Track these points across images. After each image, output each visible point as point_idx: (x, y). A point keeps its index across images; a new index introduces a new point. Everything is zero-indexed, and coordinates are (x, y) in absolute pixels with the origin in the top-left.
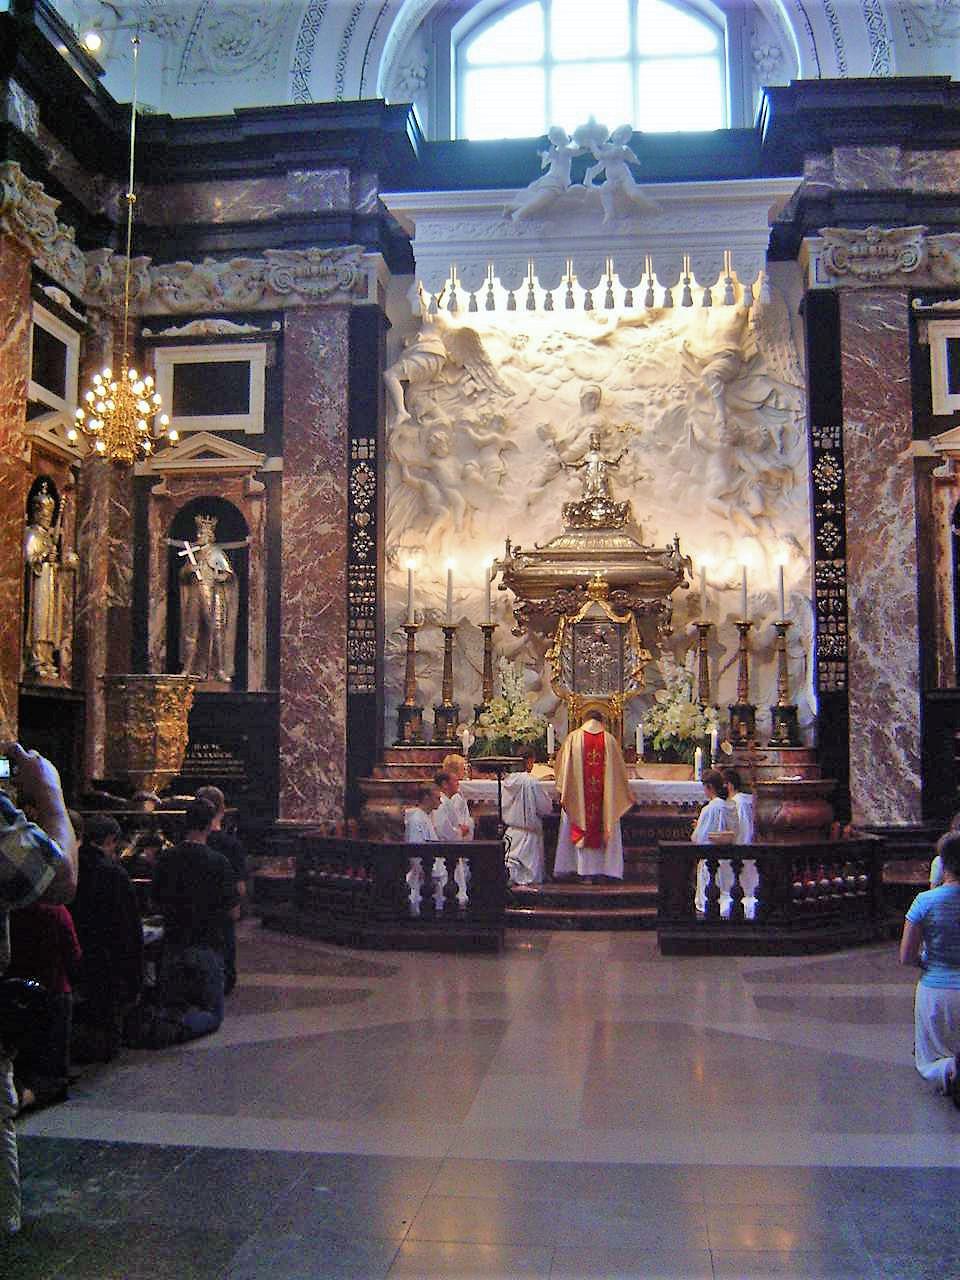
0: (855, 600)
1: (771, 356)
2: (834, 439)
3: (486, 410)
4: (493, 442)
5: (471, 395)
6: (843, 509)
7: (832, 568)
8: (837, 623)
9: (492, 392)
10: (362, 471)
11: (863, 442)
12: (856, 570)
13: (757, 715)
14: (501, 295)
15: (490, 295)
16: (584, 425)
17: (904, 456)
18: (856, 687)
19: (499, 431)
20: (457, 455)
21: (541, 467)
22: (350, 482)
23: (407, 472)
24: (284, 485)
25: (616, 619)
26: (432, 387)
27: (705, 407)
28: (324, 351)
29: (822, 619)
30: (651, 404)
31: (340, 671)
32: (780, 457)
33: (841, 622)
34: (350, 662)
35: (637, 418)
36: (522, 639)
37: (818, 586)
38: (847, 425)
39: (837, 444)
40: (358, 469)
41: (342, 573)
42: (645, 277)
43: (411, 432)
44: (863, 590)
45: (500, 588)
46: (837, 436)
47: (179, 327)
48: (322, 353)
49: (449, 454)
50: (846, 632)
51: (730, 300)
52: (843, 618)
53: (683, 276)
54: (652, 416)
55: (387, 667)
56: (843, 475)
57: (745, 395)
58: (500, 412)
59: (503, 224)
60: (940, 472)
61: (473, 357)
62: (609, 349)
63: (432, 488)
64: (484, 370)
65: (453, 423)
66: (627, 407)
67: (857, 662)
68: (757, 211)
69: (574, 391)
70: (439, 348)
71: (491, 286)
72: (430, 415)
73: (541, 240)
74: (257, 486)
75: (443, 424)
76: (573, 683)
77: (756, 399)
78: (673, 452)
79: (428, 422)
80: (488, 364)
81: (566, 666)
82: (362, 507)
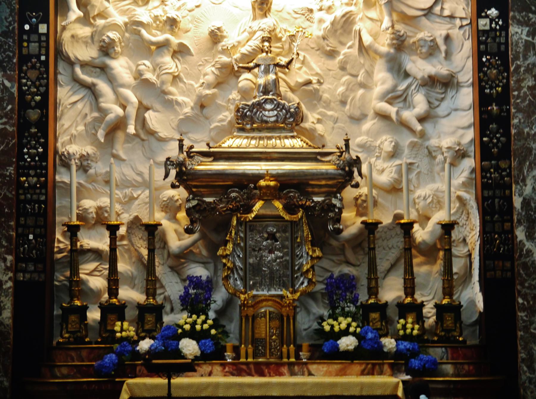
0: (521, 199)
2: (500, 44)
3: (159, 12)
4: (163, 45)
6: (509, 111)
7: (497, 168)
8: (503, 222)
10: (33, 67)
11: (528, 45)
12: (521, 170)
13: (425, 311)
16: (255, 28)
18: (522, 284)
19: (172, 32)
20: (130, 57)
21: (213, 69)
22: (20, 78)
25: (287, 217)
27: (373, 14)
29: (488, 218)
30: (321, 10)
31: (7, 269)
32: (444, 63)
33: (508, 221)
34: (18, 259)
35: (308, 23)
36: (195, 236)
37: (485, 186)
38: (513, 29)
39: (503, 48)
41: (11, 170)
43: (85, 31)
44: (528, 190)
45: (173, 186)
46: (503, 40)
49: (122, 54)
50: (512, 231)
52: (509, 217)
54: (321, 21)
55: (57, 267)
56: (508, 78)
58: (172, 14)
63: (103, 86)
65: (126, 24)
66: (296, 13)
67: (523, 260)
72: (102, 15)
75: (116, 24)
76: (244, 280)
77: (423, 6)
78: (341, 57)
79: (100, 22)
81: (239, 264)
82: (33, 103)
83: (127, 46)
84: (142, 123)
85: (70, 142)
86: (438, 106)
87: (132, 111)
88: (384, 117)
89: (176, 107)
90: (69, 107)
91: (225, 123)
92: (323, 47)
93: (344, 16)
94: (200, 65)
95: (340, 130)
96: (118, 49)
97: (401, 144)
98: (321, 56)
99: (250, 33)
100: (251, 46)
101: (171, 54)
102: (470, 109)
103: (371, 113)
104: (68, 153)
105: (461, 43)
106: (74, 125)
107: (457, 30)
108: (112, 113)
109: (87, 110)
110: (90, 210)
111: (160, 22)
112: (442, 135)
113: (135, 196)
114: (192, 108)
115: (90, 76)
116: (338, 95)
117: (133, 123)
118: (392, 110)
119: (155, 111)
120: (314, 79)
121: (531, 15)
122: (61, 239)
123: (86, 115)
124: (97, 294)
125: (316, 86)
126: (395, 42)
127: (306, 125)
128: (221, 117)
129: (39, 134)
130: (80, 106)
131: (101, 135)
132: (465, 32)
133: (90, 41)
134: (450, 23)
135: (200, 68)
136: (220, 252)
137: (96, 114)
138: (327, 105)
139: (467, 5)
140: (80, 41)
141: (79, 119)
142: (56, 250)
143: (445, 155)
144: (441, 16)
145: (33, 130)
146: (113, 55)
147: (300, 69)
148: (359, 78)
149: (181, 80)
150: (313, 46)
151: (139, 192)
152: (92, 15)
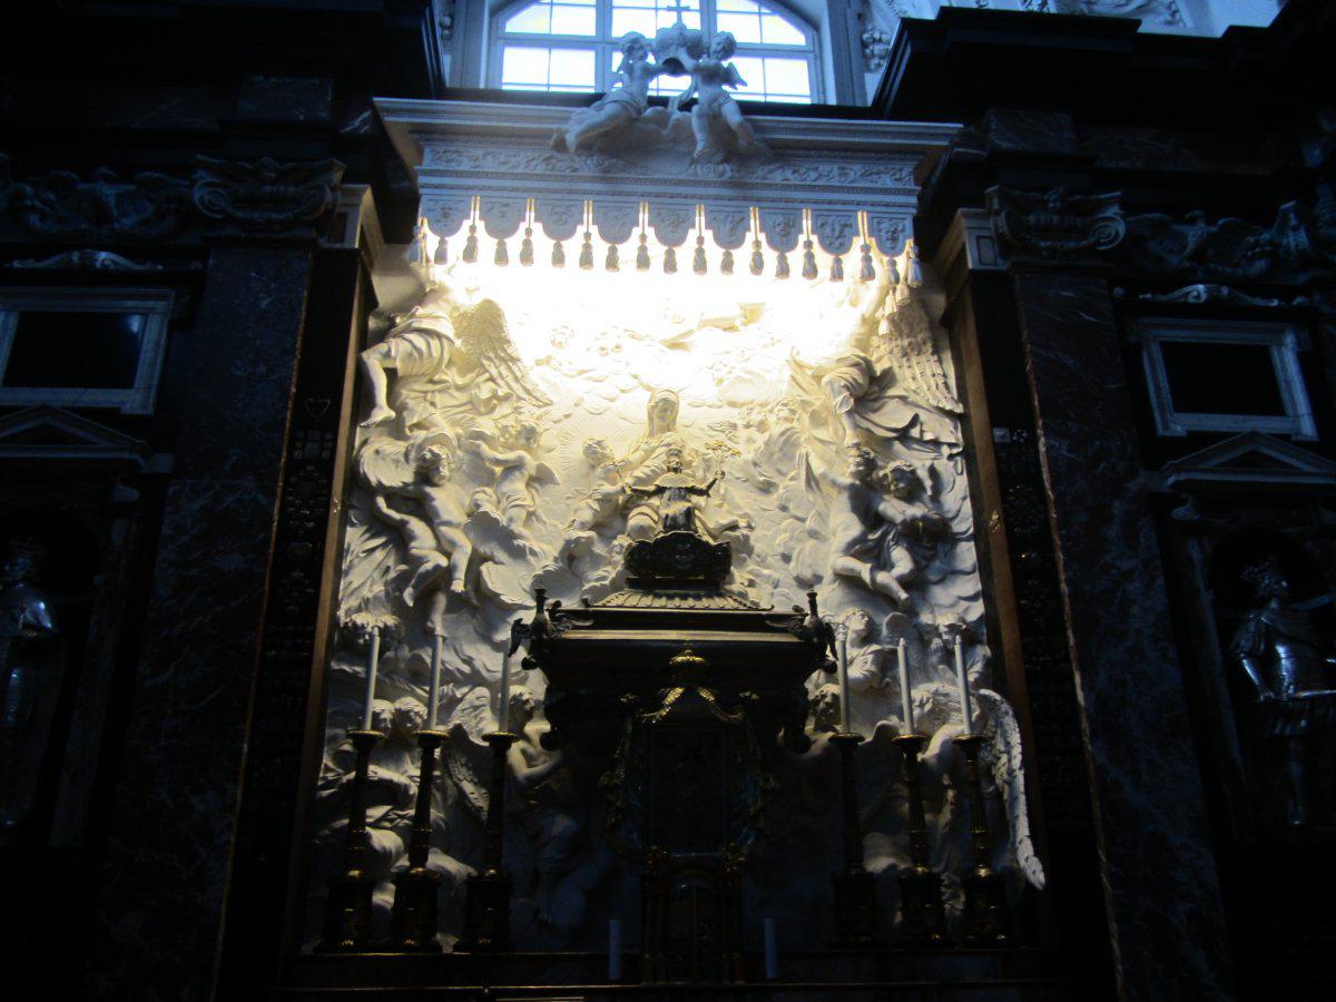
1: (908, 373)
4: (512, 468)
5: (489, 400)
9: (519, 398)
14: (543, 244)
15: (527, 244)
17: (1133, 486)
21: (590, 501)
23: (381, 502)
24: (171, 490)
26: (430, 387)
28: (268, 301)
40: (302, 474)
42: (750, 237)
47: (39, 260)
48: (264, 304)
51: (868, 274)
53: (802, 238)
57: (875, 417)
59: (550, 158)
60: (1179, 513)
61: (494, 350)
62: (685, 353)
63: (416, 526)
64: (509, 368)
68: (898, 167)
69: (638, 406)
70: (446, 327)
71: (529, 232)
73: (603, 180)
74: (130, 494)
77: (894, 425)
80: (515, 360)
83: (459, 469)
84: (474, 576)
85: (359, 610)
86: (927, 567)
87: (462, 560)
88: (849, 580)
89: (529, 557)
90: (362, 555)
91: (607, 582)
92: (754, 477)
93: (782, 434)
94: (568, 498)
95: (784, 598)
96: (445, 471)
97: (877, 620)
98: (751, 489)
99: (646, 451)
100: (648, 467)
101: (526, 479)
102: (973, 572)
103: (828, 575)
104: (355, 624)
105: (952, 479)
106: (369, 582)
107: (945, 461)
108: (428, 561)
109: (391, 562)
110: (383, 716)
111: (511, 436)
112: (936, 609)
113: (459, 695)
114: (556, 560)
115: (398, 511)
116: (779, 545)
117: (463, 577)
118: (864, 569)
119: (496, 563)
120: (742, 523)
121: (1069, 423)
122: (330, 764)
123: (388, 569)
124: (385, 857)
125: (745, 532)
126: (861, 468)
127: (735, 587)
128: (600, 573)
129: (307, 582)
130: (379, 555)
131: (408, 596)
132: (956, 463)
133: (403, 460)
134: (934, 451)
135: (568, 502)
136: (604, 780)
137: (403, 567)
138: (763, 562)
139: (956, 428)
140: (388, 459)
141: (376, 575)
142: (320, 783)
143: (945, 637)
144: (920, 441)
145: (298, 574)
146: (436, 480)
147: (720, 506)
148: (808, 522)
149: (538, 519)
150: (738, 475)
151: (465, 690)
152: (408, 423)
